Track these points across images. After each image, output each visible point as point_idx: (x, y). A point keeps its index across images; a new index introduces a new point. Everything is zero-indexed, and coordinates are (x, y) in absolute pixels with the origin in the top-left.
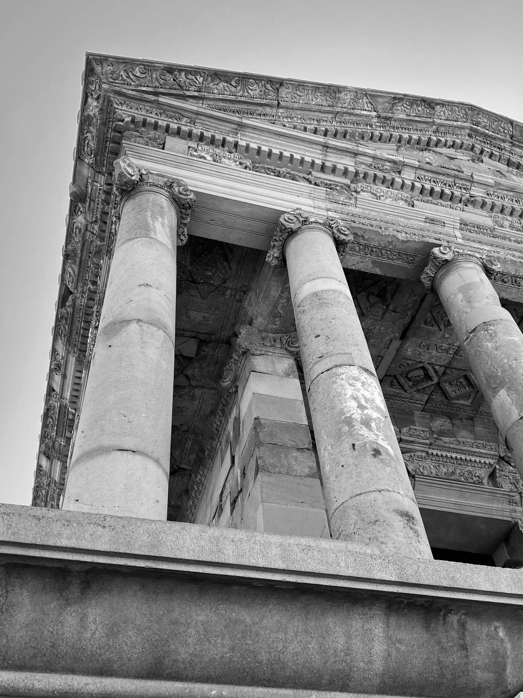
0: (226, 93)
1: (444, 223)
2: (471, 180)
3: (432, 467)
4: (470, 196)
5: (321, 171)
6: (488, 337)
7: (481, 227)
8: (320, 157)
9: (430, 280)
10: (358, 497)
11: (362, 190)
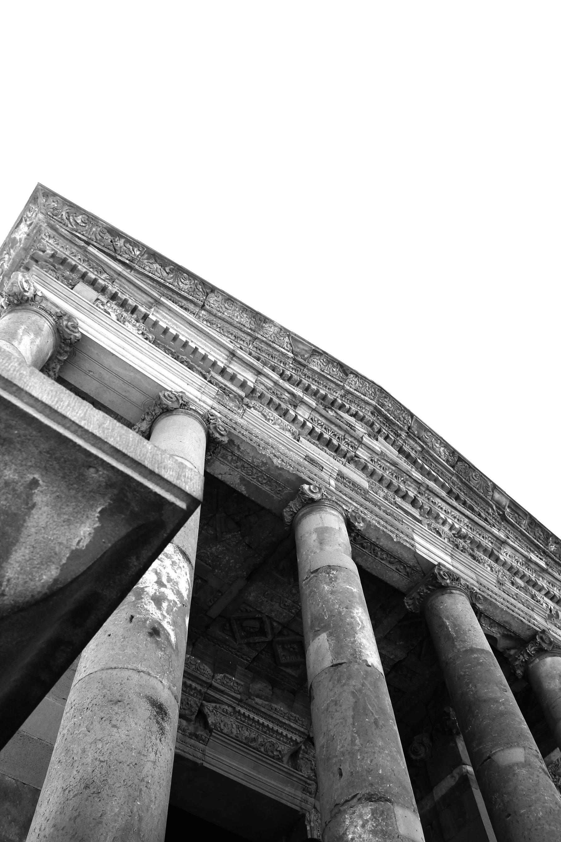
0: (156, 274)
1: (323, 468)
2: (360, 442)
3: (234, 726)
4: (355, 456)
5: (220, 374)
6: (328, 580)
7: (356, 485)
8: (225, 361)
9: (291, 515)
10: (110, 671)
11: (253, 407)
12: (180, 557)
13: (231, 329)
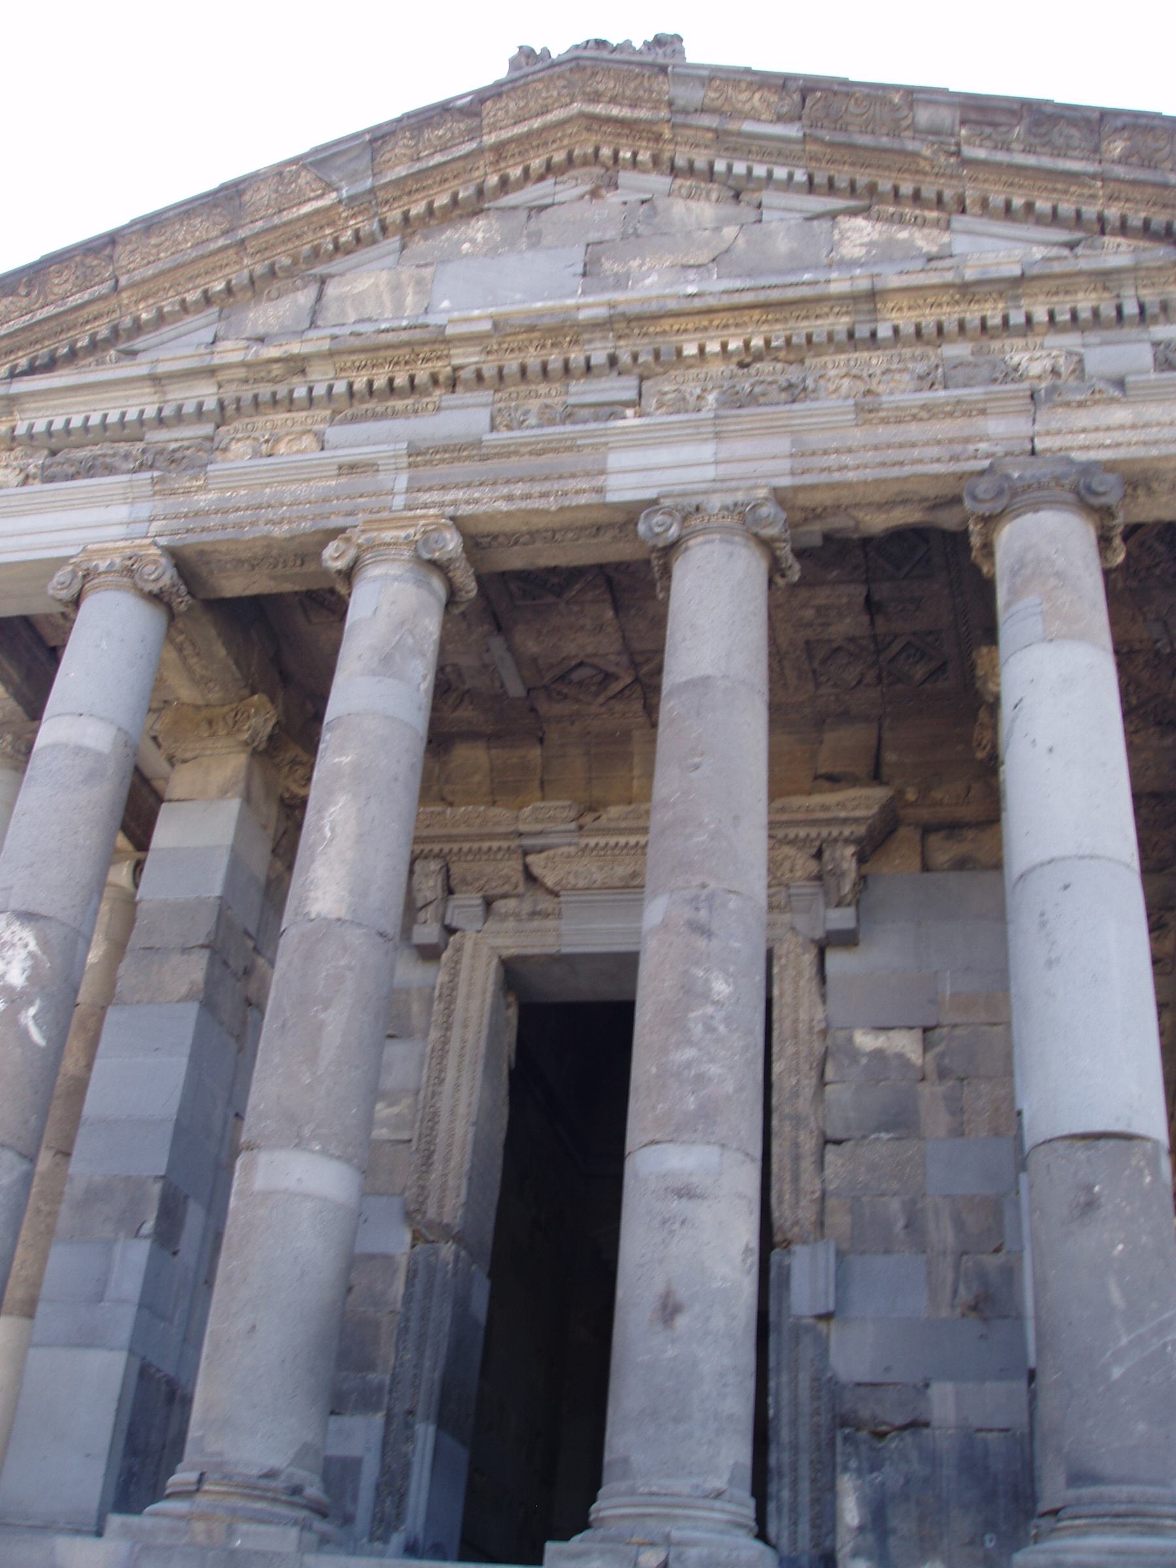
1: (375, 464)
3: (594, 869)
8: (155, 398)
12: (16, 927)
13: (190, 271)
